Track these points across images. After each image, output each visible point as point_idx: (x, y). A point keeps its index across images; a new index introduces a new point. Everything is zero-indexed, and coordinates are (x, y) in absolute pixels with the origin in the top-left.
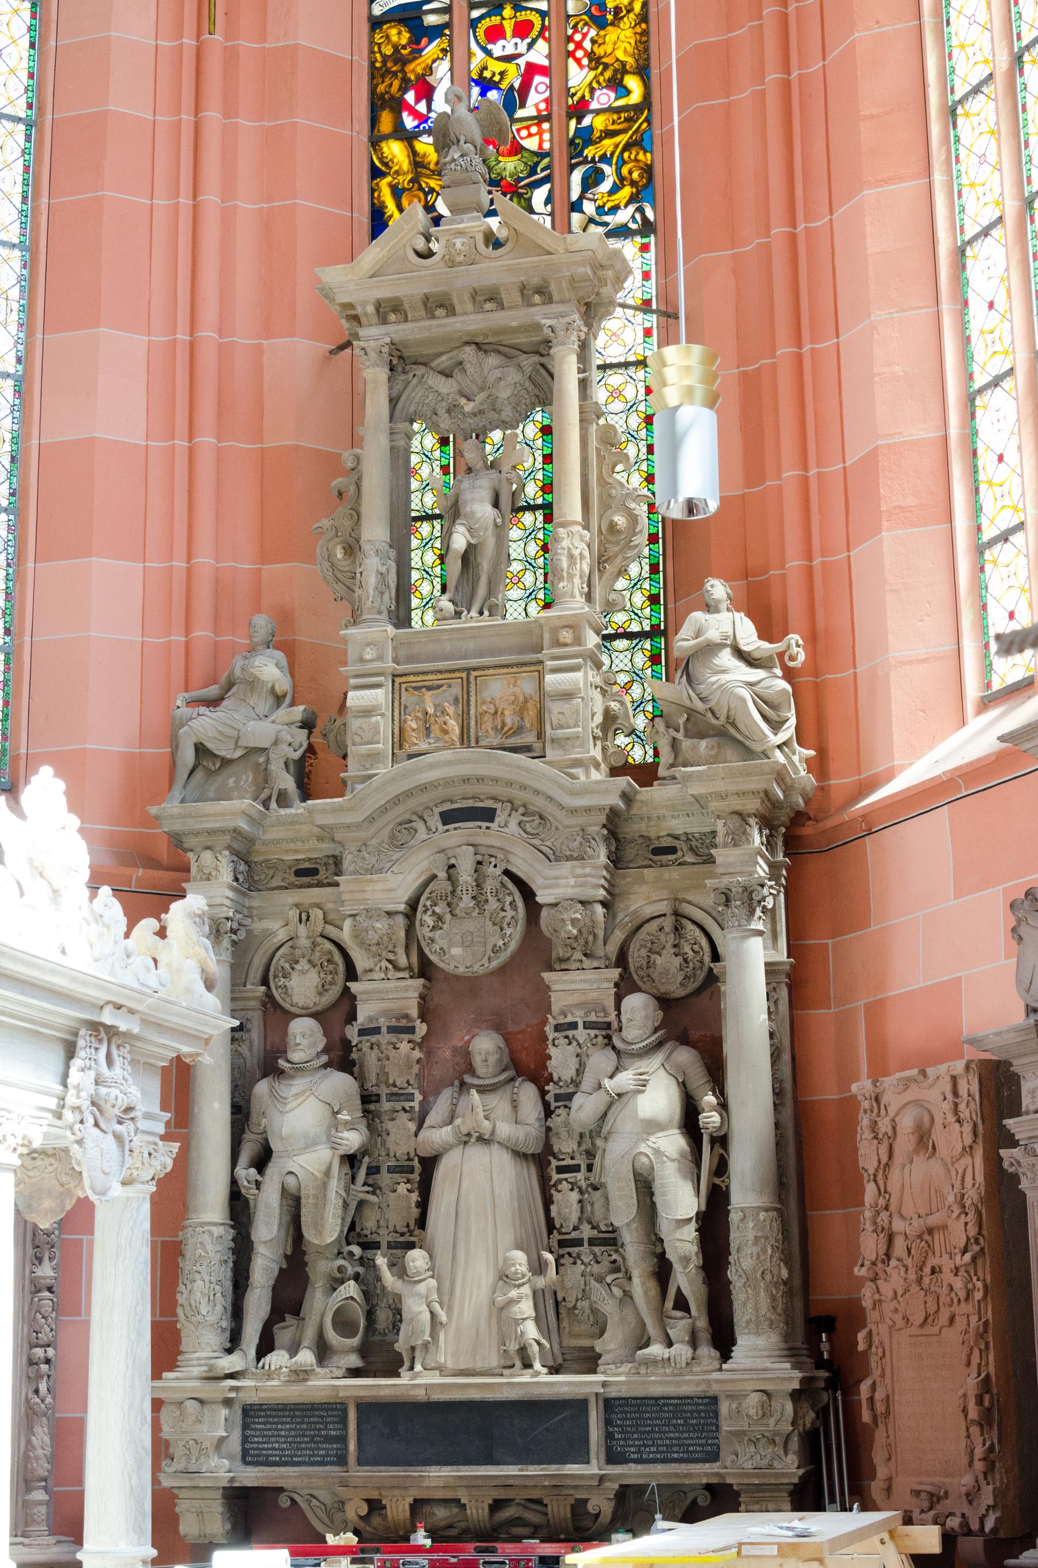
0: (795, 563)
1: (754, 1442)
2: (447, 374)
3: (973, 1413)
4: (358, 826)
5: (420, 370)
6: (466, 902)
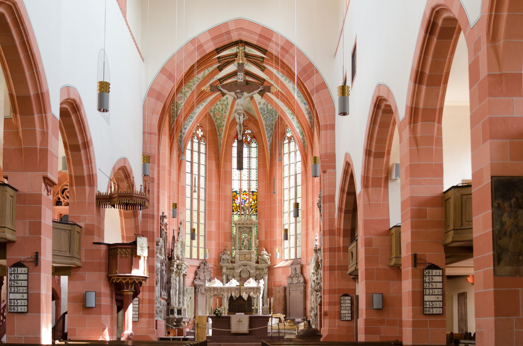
0: (269, 247)
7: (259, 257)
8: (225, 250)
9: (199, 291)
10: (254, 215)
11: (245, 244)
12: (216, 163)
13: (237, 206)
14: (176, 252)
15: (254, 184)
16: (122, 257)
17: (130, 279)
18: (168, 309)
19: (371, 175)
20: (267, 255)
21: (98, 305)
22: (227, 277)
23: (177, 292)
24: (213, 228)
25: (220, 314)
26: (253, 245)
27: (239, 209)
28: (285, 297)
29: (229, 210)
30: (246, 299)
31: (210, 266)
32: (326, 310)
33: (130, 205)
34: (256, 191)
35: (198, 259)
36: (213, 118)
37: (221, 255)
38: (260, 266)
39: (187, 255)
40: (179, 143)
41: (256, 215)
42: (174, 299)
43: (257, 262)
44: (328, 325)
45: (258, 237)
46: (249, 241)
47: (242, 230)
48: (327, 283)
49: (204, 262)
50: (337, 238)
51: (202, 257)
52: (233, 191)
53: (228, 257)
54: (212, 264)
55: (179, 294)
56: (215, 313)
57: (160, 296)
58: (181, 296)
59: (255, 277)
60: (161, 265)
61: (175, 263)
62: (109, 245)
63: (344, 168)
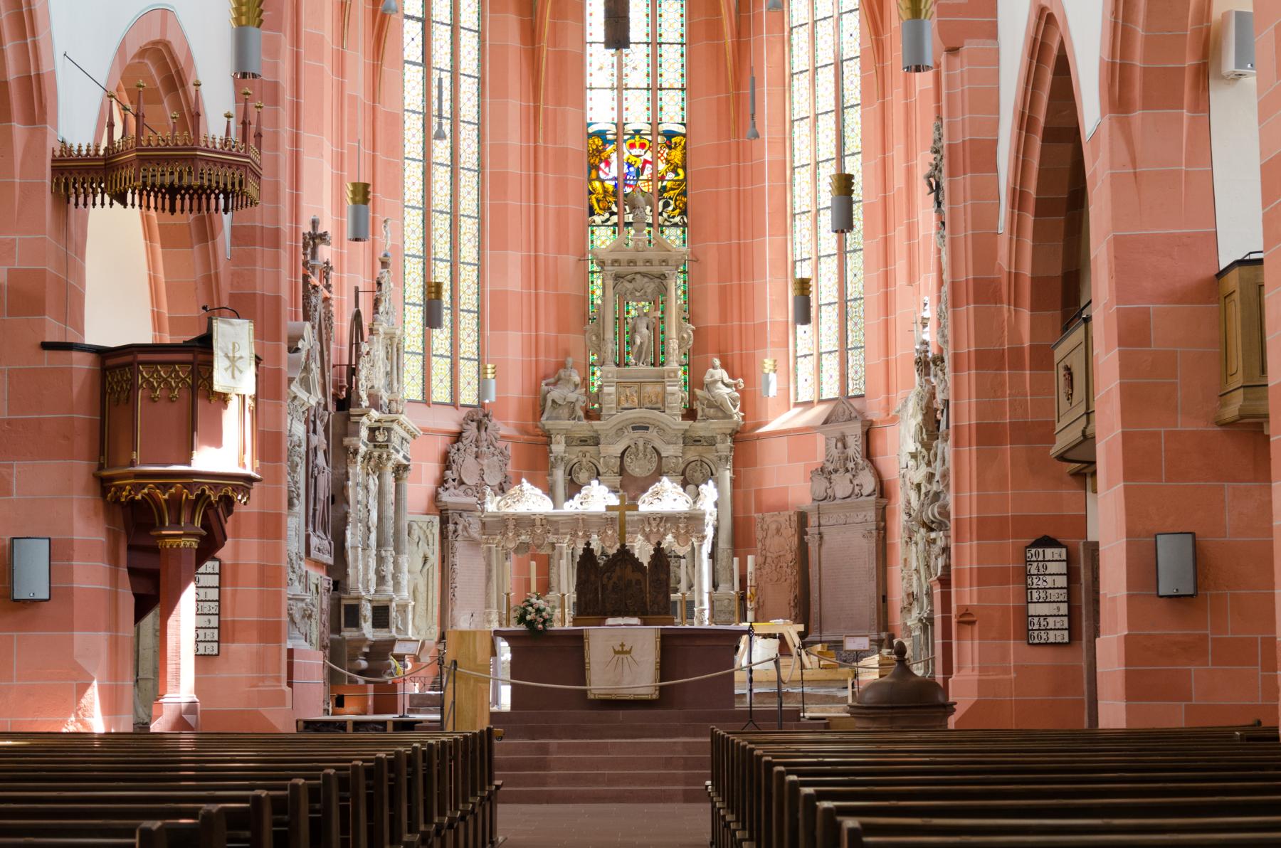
0: (737, 352)
1: (725, 613)
2: (631, 282)
3: (792, 604)
4: (606, 430)
5: (622, 280)
6: (641, 455)
7: (698, 392)
8: (562, 365)
9: (460, 531)
10: (676, 225)
11: (638, 341)
12: (522, 23)
13: (605, 191)
14: (367, 379)
15: (672, 103)
16: (153, 400)
17: (186, 486)
18: (336, 605)
19: (1138, 61)
20: (727, 385)
21: (60, 592)
22: (570, 474)
23: (373, 536)
24: (514, 281)
25: (544, 623)
26: (674, 344)
27: (616, 203)
28: (803, 549)
29: (576, 207)
30: (645, 561)
31: (502, 432)
32: (968, 603)
33: (187, 192)
34: (682, 130)
35: (454, 404)
37: (544, 388)
38: (699, 428)
39: (412, 389)
41: (685, 225)
42: (361, 567)
43: (690, 414)
44: (976, 665)
45: (690, 315)
46: (658, 330)
47: (629, 286)
48: (970, 494)
49: (479, 417)
50: (1006, 315)
51: (468, 396)
52: (590, 130)
53: (572, 397)
54: (511, 421)
55: (380, 544)
56: (521, 619)
57: (303, 554)
58: (389, 553)
59: (683, 473)
60: (308, 432)
61: (364, 419)
62: (102, 353)
63: (1032, 33)
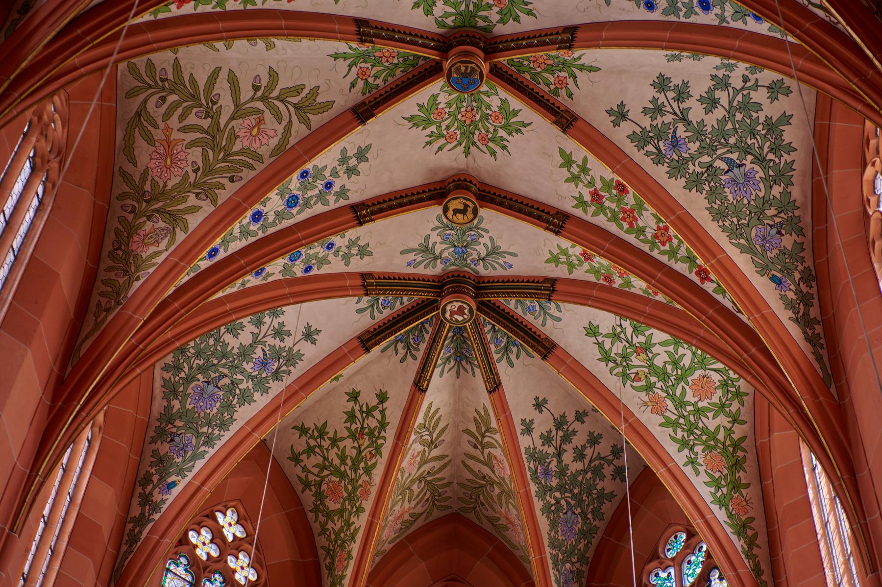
36: (311, 516)
40: (124, 548)
